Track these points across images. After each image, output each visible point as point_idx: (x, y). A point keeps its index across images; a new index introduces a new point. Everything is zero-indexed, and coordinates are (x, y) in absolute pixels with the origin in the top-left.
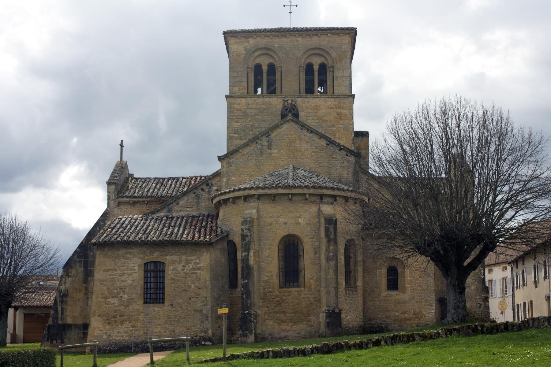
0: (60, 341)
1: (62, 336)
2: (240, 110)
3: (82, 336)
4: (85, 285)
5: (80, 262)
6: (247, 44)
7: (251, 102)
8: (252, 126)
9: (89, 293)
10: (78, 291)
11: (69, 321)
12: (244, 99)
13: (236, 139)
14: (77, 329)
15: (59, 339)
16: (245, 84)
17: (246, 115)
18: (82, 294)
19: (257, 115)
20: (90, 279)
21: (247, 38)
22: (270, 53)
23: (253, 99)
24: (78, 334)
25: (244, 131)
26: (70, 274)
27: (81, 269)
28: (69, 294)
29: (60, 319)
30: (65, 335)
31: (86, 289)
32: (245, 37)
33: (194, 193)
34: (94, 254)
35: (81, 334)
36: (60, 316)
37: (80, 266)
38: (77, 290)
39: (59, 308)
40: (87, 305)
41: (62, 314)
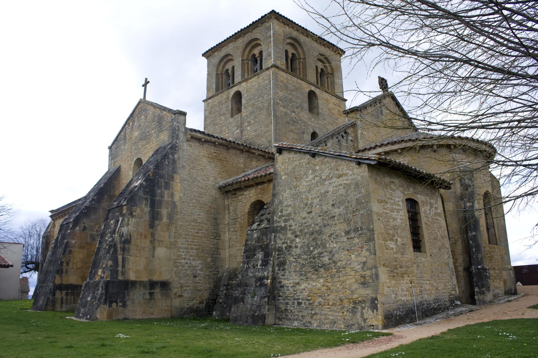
0: (121, 304)
1: (124, 297)
2: (282, 82)
3: (148, 297)
4: (151, 230)
5: (146, 199)
6: (284, 29)
7: (289, 78)
8: (291, 99)
9: (156, 241)
10: (143, 237)
11: (132, 277)
12: (284, 73)
13: (281, 106)
14: (142, 288)
15: (120, 302)
16: (284, 61)
17: (286, 88)
18: (147, 242)
19: (293, 90)
20: (157, 222)
21: (284, 24)
22: (296, 45)
23: (291, 76)
24: (144, 294)
25: (286, 101)
26: (134, 214)
27: (147, 209)
28: (133, 240)
29: (120, 274)
30: (128, 295)
31: (153, 235)
32: (284, 23)
33: (337, 138)
34: (162, 192)
35: (147, 295)
36: (120, 269)
37: (146, 205)
38: (141, 235)
39: (120, 258)
40: (153, 257)
41: (123, 266)
